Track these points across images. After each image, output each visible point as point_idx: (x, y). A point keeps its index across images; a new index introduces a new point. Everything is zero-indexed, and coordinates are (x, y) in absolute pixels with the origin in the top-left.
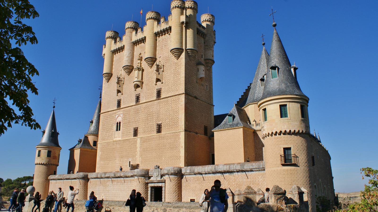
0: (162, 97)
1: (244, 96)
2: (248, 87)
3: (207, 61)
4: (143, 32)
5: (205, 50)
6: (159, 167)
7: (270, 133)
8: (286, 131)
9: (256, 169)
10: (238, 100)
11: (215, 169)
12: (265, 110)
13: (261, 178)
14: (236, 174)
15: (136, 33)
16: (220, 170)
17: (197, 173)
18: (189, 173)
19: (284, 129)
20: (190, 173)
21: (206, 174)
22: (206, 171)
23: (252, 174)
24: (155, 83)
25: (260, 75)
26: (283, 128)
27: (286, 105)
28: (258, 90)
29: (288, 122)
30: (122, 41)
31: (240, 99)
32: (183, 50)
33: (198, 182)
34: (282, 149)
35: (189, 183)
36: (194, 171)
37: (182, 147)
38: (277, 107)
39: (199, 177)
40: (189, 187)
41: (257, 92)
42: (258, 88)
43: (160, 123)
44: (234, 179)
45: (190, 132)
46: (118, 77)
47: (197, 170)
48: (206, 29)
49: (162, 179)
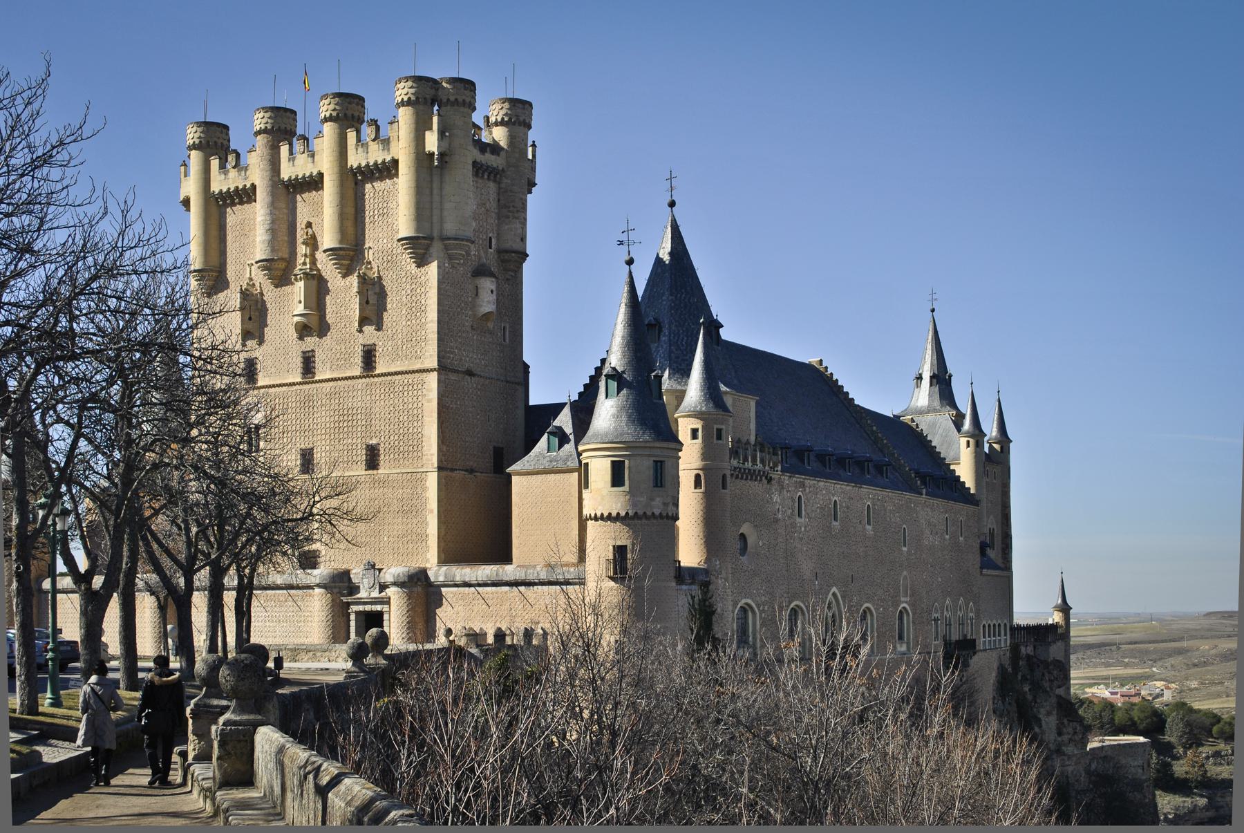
0: (377, 372)
2: (596, 369)
3: (507, 256)
4: (313, 156)
5: (499, 219)
6: (373, 566)
12: (587, 464)
15: (291, 153)
24: (356, 324)
30: (246, 169)
32: (431, 238)
37: (432, 511)
38: (607, 463)
43: (374, 442)
45: (452, 470)
46: (241, 292)
48: (502, 153)
49: (383, 594)
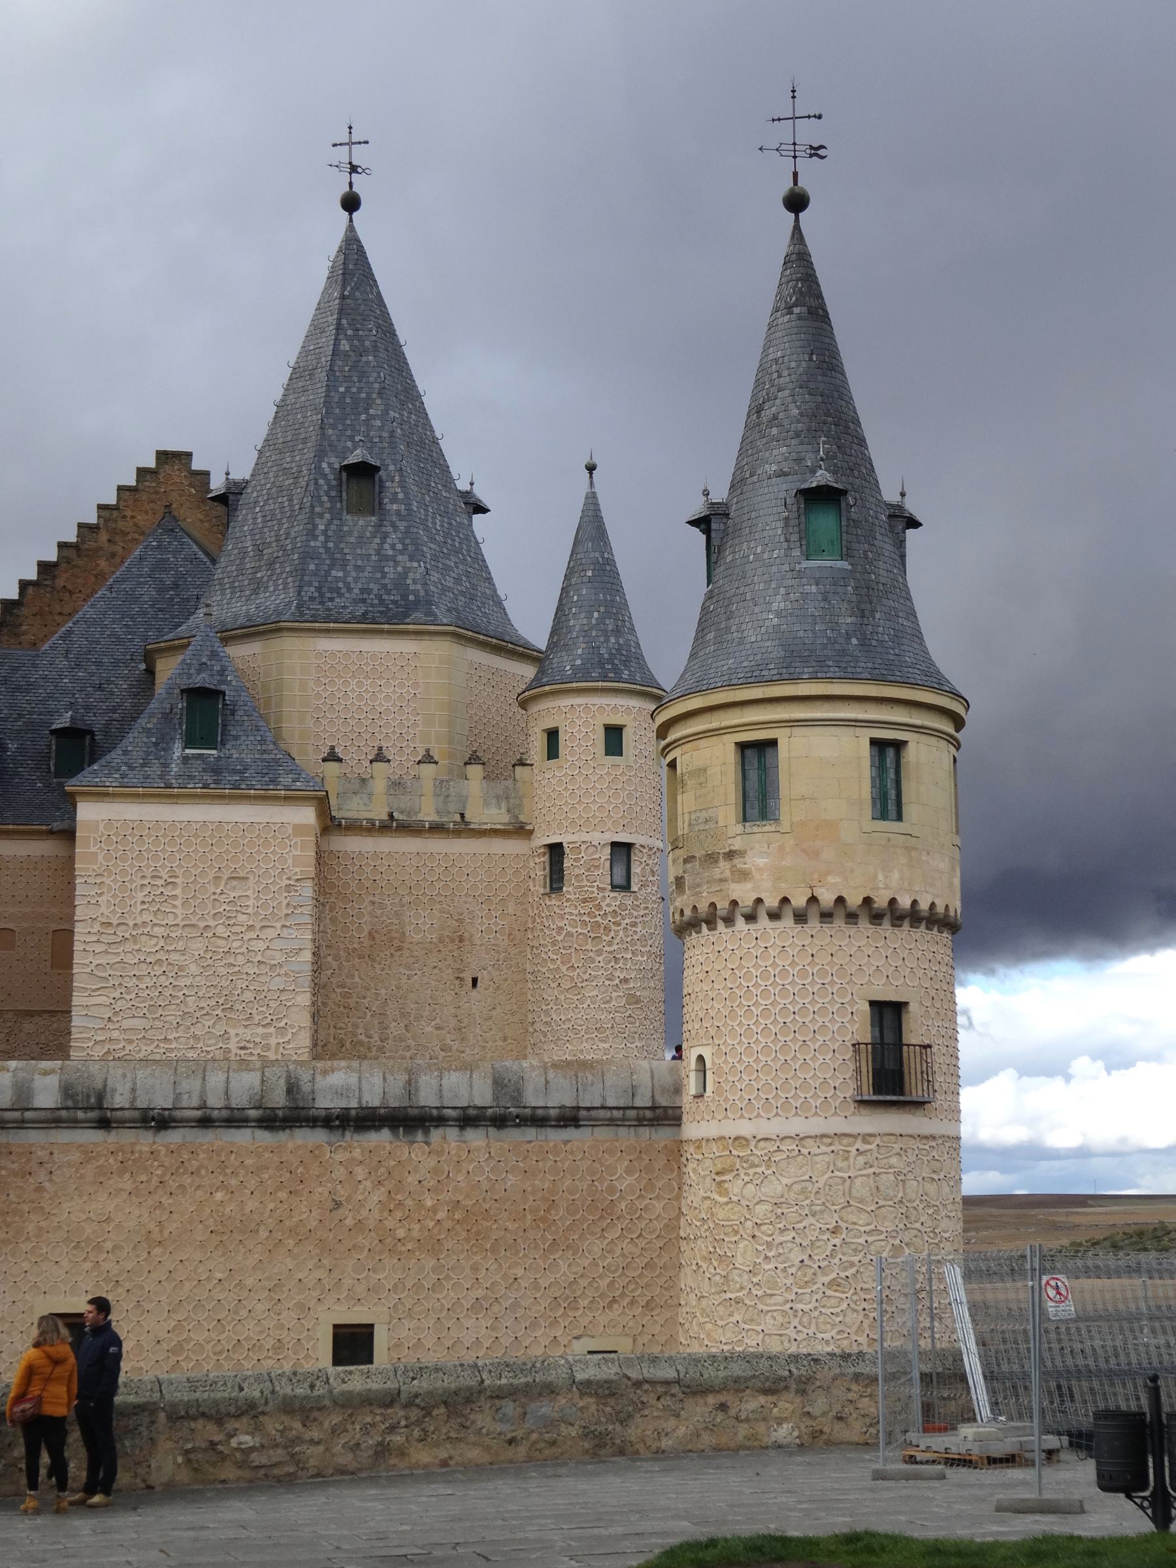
1: (104, 536)
7: (799, 901)
8: (893, 901)
9: (602, 1113)
10: (52, 556)
11: (289, 1091)
13: (628, 1171)
14: (448, 1138)
16: (325, 1102)
17: (127, 1114)
18: (48, 1114)
19: (887, 887)
20: (67, 1108)
21: (205, 1122)
22: (215, 1101)
23: (566, 1142)
25: (333, 426)
26: (881, 885)
27: (899, 746)
28: (325, 532)
29: (906, 848)
31: (62, 546)
33: (128, 1186)
34: (867, 1007)
35: (40, 1189)
36: (101, 1097)
38: (858, 746)
39: (134, 1144)
40: (33, 1217)
41: (322, 550)
42: (325, 521)
44: (435, 1171)
47: (134, 1090)
